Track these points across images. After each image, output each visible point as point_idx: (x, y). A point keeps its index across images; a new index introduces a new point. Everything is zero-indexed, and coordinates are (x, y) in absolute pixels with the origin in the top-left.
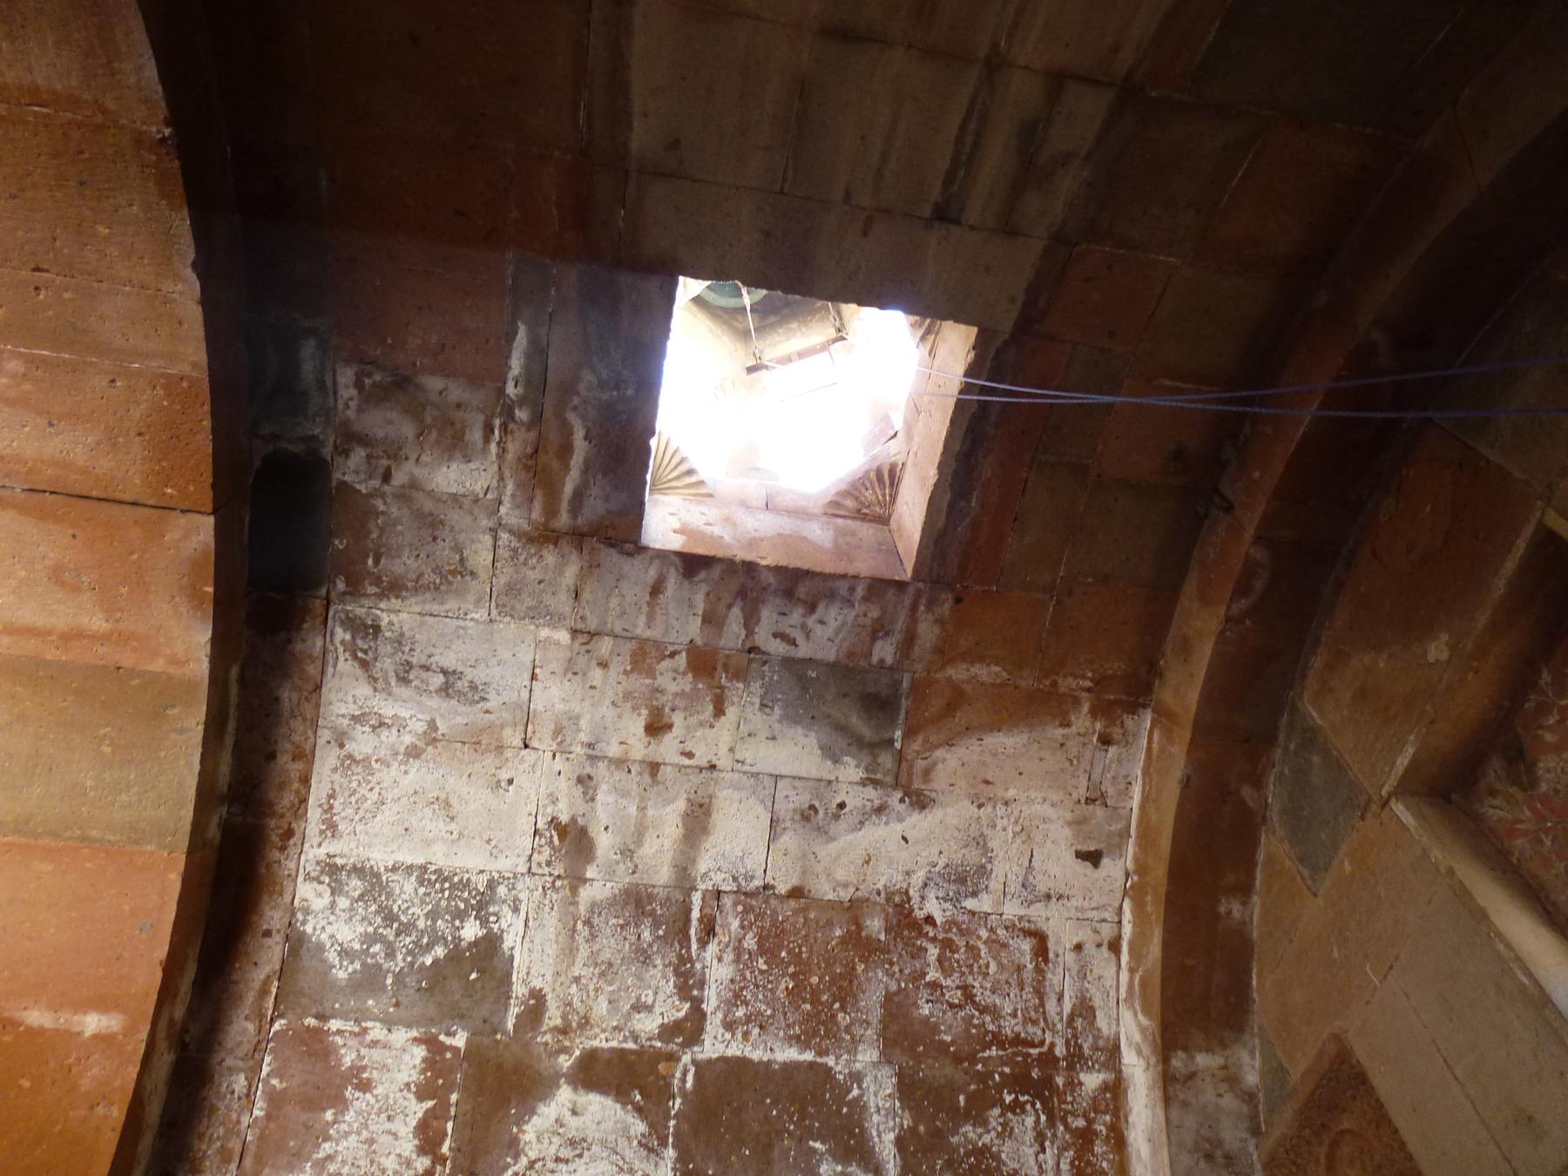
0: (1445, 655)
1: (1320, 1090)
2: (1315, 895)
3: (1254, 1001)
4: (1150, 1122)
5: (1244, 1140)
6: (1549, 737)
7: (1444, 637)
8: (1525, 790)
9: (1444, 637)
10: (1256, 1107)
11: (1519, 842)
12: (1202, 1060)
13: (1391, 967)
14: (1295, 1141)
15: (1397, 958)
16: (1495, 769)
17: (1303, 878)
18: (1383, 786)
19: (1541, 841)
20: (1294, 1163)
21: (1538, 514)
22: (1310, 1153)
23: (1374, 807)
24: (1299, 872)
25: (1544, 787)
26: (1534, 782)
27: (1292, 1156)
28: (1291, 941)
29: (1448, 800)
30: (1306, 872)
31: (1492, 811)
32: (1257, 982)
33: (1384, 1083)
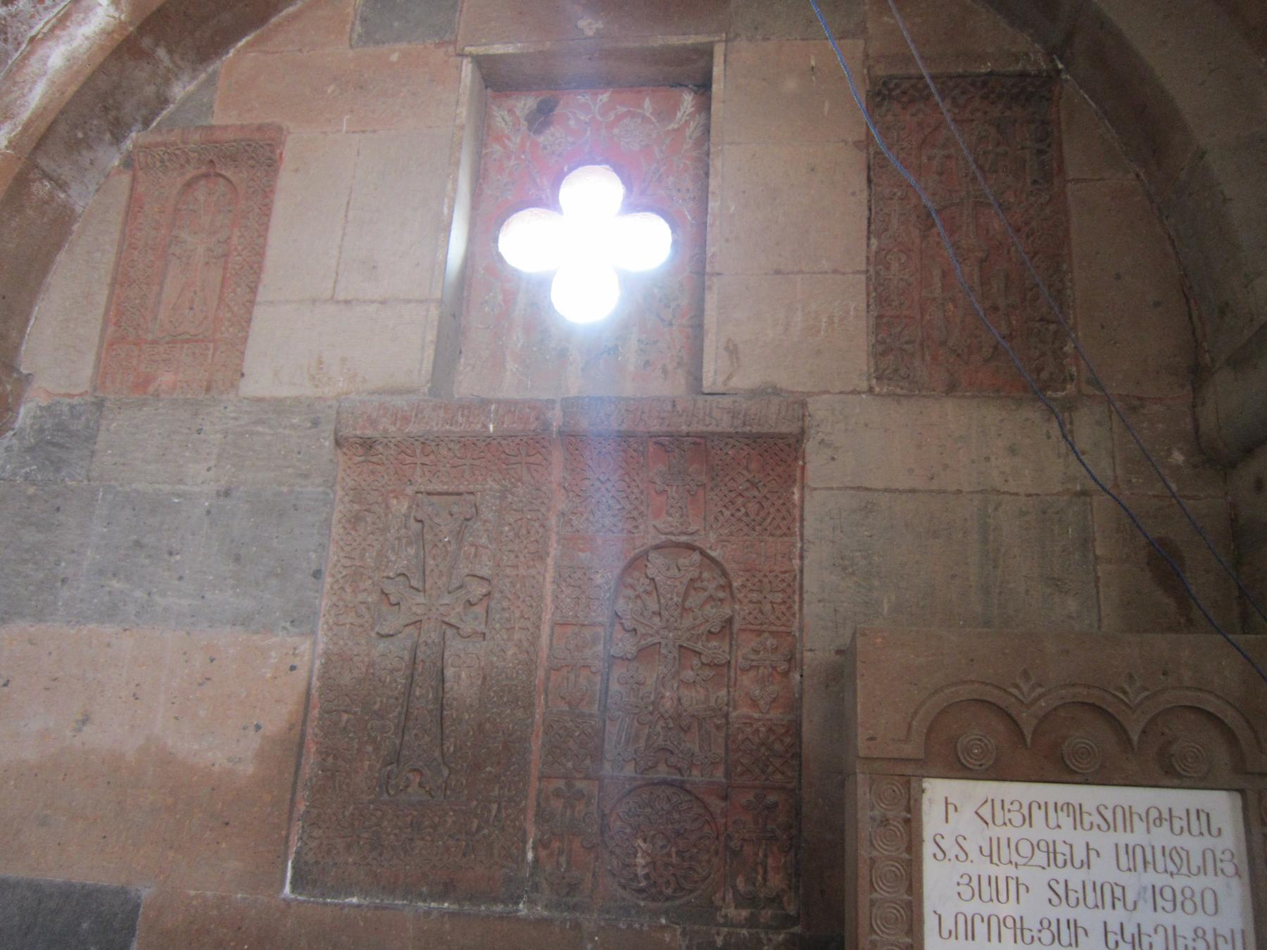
0: (590, 33)
1: (235, 144)
2: (351, 47)
3: (227, 53)
4: (81, 50)
5: (136, 121)
6: (572, 123)
7: (600, 25)
8: (530, 130)
9: (600, 25)
10: (163, 109)
11: (497, 148)
12: (161, 53)
13: (364, 132)
14: (177, 152)
15: (374, 131)
16: (525, 104)
17: (352, 30)
18: (471, 46)
19: (509, 158)
20: (162, 161)
21: (717, 39)
22: (182, 166)
23: (451, 49)
24: (353, 24)
25: (541, 139)
26: (539, 132)
27: (166, 157)
28: (300, 50)
29: (486, 87)
30: (359, 29)
31: (499, 119)
32: (242, 46)
33: (285, 179)
